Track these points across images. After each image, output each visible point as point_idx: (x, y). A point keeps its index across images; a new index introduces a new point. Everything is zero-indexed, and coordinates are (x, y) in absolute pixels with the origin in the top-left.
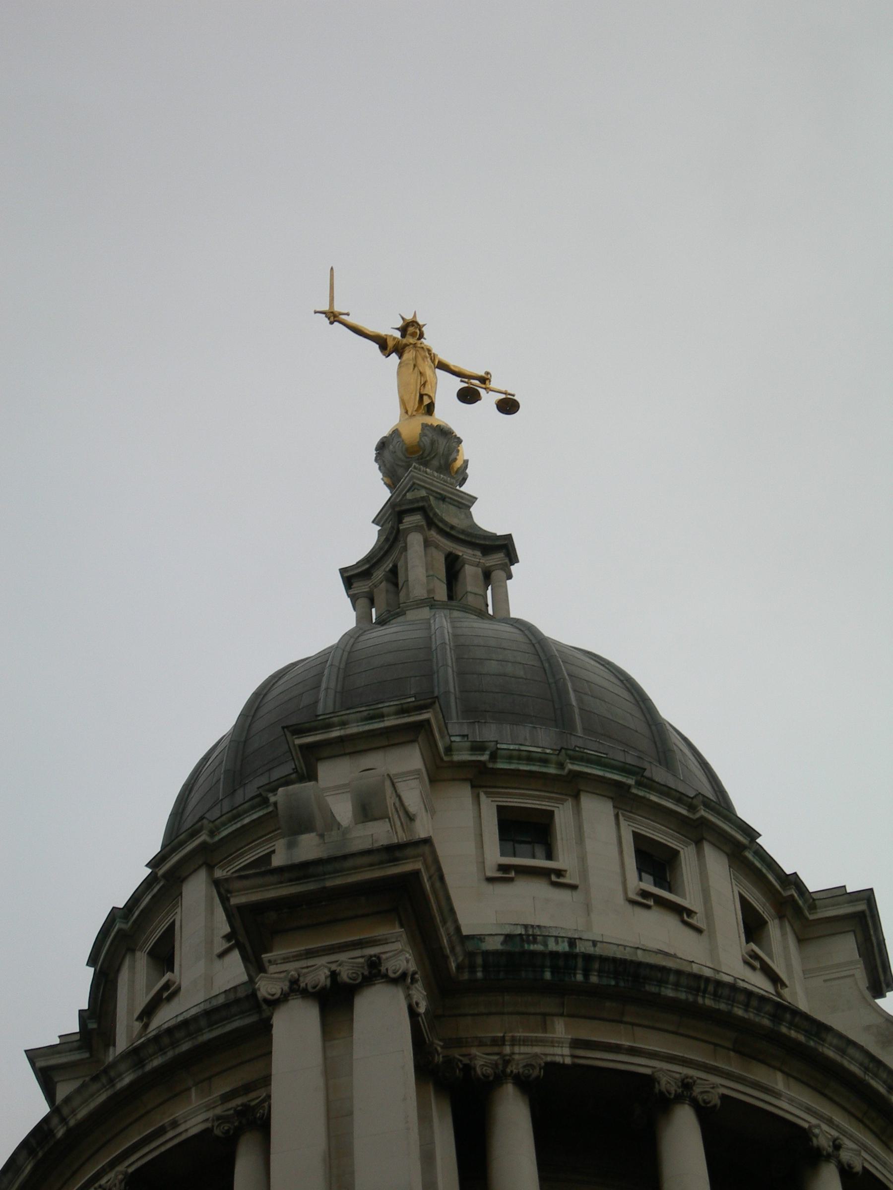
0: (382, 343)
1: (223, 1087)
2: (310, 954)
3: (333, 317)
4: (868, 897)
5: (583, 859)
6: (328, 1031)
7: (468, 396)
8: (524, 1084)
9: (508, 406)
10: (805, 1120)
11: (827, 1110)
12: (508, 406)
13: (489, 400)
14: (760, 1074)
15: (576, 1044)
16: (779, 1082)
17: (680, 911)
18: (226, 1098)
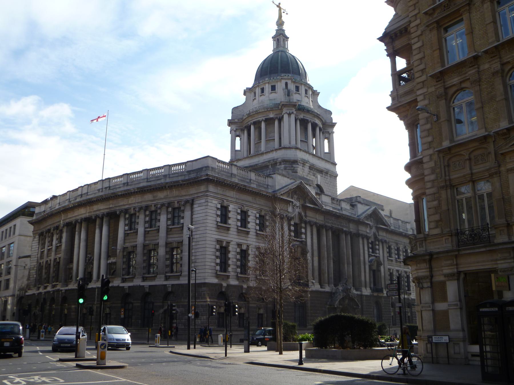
0: (277, 6)
1: (275, 113)
2: (287, 110)
3: (273, 2)
5: (302, 92)
6: (288, 117)
7: (284, 12)
8: (299, 120)
9: (287, 14)
10: (317, 123)
12: (287, 14)
13: (286, 13)
15: (304, 116)
16: (316, 119)
17: (308, 97)
18: (275, 115)
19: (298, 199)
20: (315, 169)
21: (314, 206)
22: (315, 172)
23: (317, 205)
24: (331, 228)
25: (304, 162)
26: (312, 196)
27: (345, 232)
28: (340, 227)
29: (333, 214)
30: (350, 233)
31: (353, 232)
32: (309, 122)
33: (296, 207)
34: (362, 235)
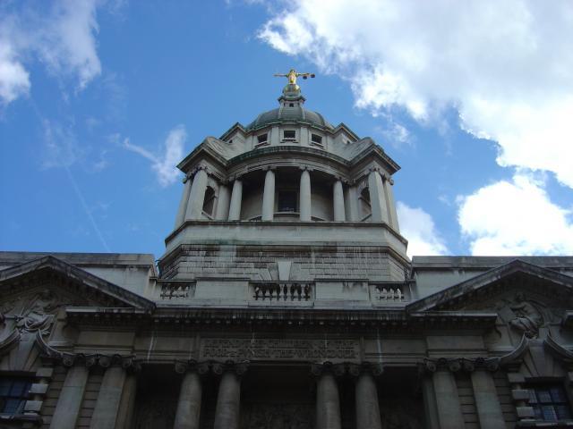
4: (342, 124)
8: (239, 179)
9: (313, 76)
11: (301, 161)
12: (313, 76)
13: (309, 77)
14: (289, 160)
19: (47, 310)
20: (265, 251)
21: (103, 310)
22: (264, 259)
23: (125, 305)
24: (230, 367)
25: (211, 249)
26: (99, 285)
27: (328, 368)
28: (296, 358)
29: (232, 319)
30: (367, 368)
31: (381, 367)
32: (265, 172)
33: (34, 327)
34: (443, 365)
